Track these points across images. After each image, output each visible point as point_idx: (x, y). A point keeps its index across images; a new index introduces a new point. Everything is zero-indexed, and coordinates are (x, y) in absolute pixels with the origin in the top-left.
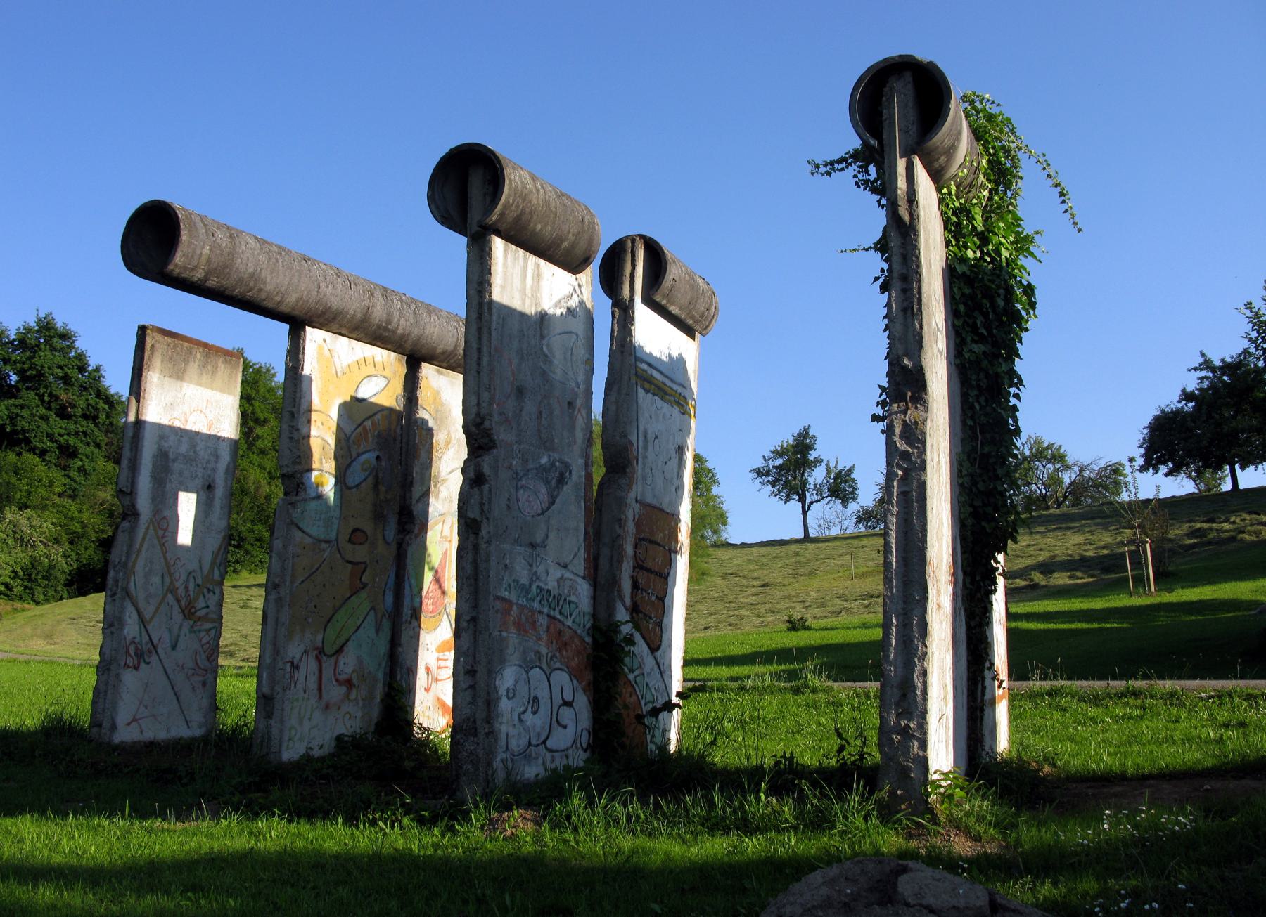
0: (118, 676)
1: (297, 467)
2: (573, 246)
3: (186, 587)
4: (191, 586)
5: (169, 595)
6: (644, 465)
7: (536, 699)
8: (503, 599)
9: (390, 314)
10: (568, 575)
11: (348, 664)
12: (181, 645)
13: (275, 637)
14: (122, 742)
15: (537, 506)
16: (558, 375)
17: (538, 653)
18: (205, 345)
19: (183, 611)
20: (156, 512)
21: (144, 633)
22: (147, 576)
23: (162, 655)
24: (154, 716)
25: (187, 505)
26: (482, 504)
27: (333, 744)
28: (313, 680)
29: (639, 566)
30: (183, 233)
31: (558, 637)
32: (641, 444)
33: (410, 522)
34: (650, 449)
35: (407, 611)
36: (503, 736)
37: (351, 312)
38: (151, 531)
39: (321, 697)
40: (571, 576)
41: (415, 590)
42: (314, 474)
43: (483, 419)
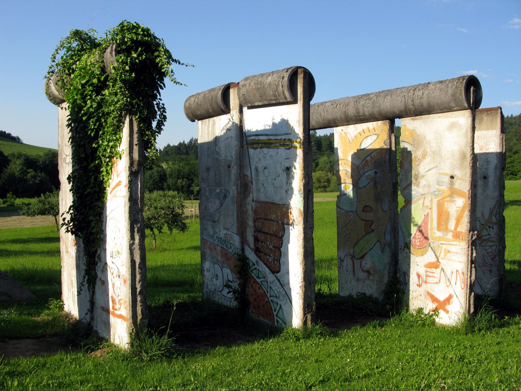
2: (213, 109)
6: (257, 185)
7: (217, 275)
8: (204, 239)
10: (228, 233)
11: (367, 263)
15: (215, 207)
16: (222, 157)
28: (350, 268)
29: (257, 230)
31: (225, 254)
32: (253, 174)
34: (261, 175)
35: (401, 244)
37: (339, 117)
39: (354, 275)
40: (231, 233)
42: (343, 185)
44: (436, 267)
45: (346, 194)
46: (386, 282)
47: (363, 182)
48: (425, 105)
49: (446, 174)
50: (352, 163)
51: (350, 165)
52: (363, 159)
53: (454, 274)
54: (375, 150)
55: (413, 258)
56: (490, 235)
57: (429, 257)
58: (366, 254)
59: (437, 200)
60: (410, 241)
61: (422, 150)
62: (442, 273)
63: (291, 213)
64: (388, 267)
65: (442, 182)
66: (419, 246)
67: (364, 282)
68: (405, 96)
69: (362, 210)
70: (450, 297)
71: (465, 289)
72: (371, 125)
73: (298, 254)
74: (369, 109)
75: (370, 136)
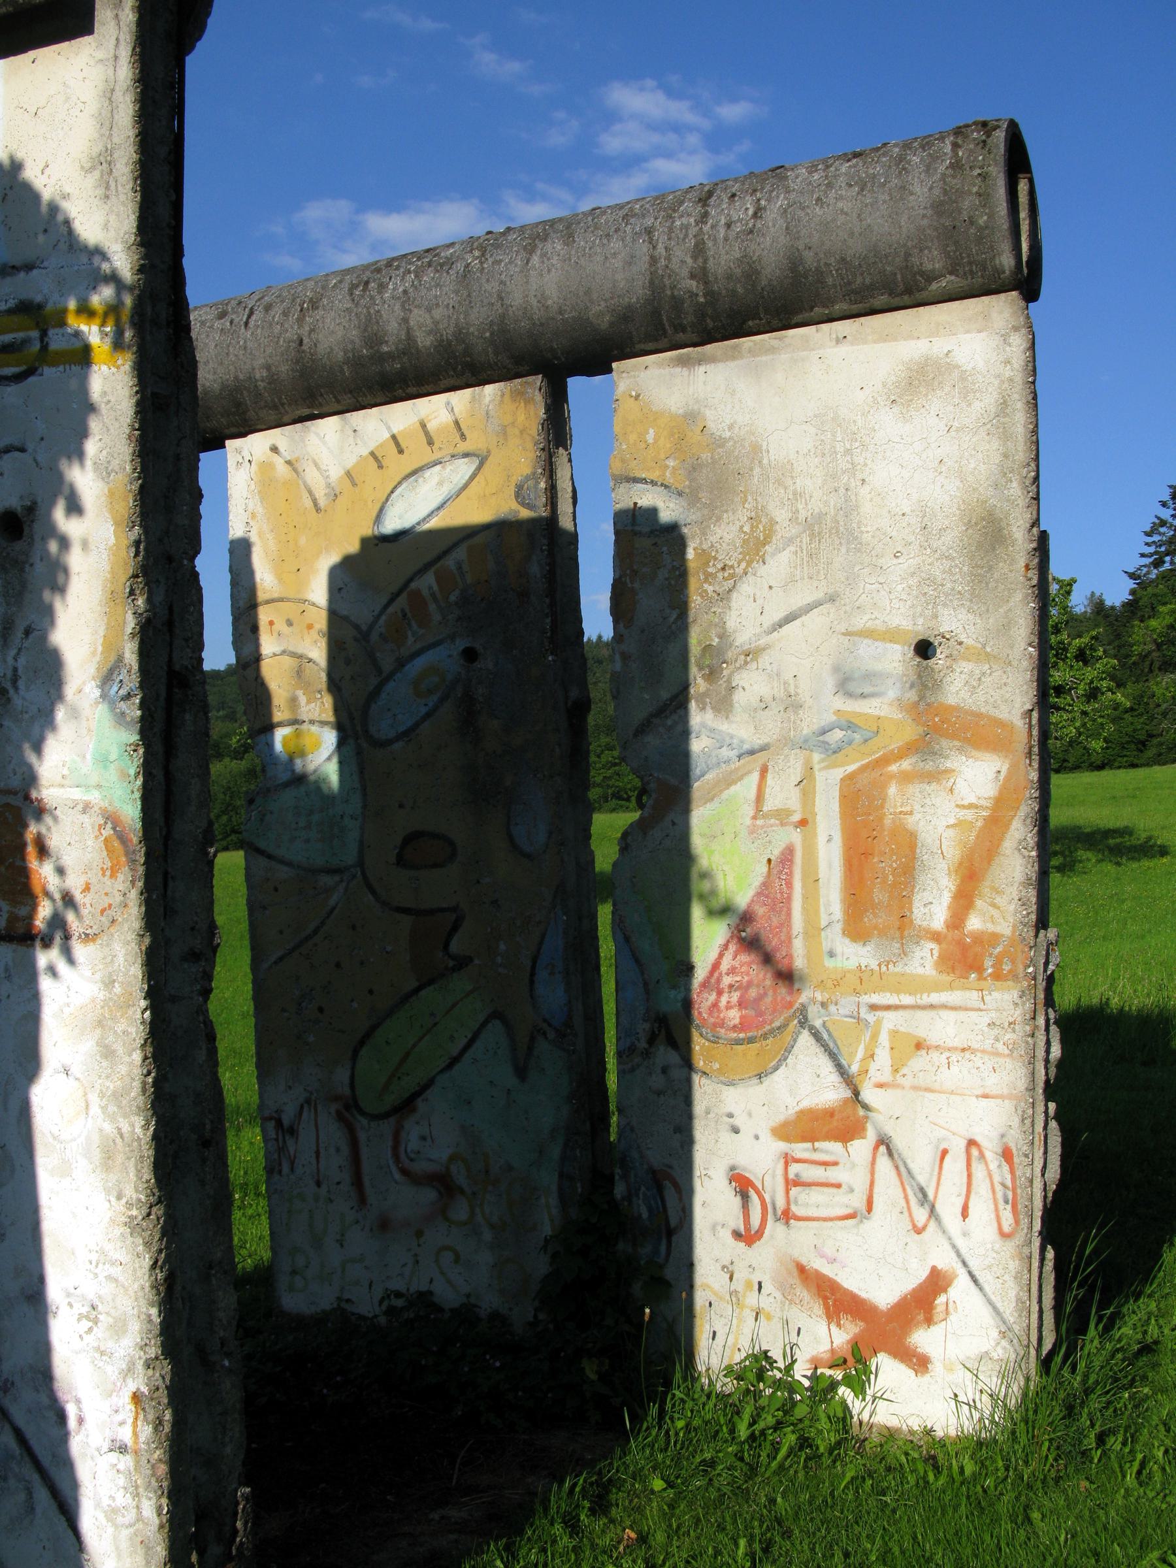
11: (435, 1136)
28: (335, 1165)
39: (362, 1200)
42: (280, 735)
45: (300, 779)
46: (547, 1230)
47: (400, 706)
48: (772, 265)
49: (891, 635)
50: (335, 615)
51: (321, 621)
52: (398, 593)
53: (955, 1166)
54: (467, 534)
55: (707, 1095)
57: (805, 1080)
59: (839, 773)
60: (687, 1004)
61: (743, 515)
62: (883, 1163)
63: (43, 851)
64: (556, 1151)
65: (869, 676)
66: (742, 1026)
67: (419, 1234)
68: (649, 231)
70: (936, 1282)
71: (1019, 1238)
72: (437, 409)
73: (108, 1156)
74: (437, 313)
75: (434, 464)
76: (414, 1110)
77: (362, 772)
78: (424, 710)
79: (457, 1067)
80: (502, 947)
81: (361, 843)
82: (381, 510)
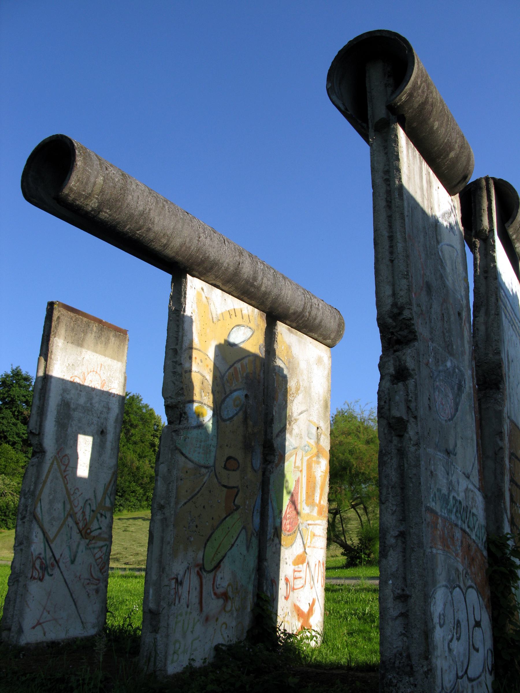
0: (25, 586)
1: (180, 398)
3: (84, 512)
4: (88, 511)
5: (70, 519)
9: (255, 272)
11: (224, 578)
12: (79, 559)
13: (161, 555)
14: (27, 644)
17: (457, 570)
18: (100, 322)
19: (80, 532)
20: (59, 450)
21: (48, 550)
22: (51, 502)
23: (62, 569)
24: (55, 620)
25: (85, 445)
26: (408, 401)
27: (213, 654)
30: (78, 158)
33: (271, 453)
35: (270, 530)
36: (439, 673)
37: (225, 265)
38: (55, 466)
39: (201, 610)
41: (277, 512)
42: (195, 405)
43: (401, 309)
44: (302, 562)
51: (211, 366)
56: (100, 528)
58: (224, 557)
67: (217, 620)
69: (223, 465)
76: (220, 567)
77: (218, 428)
78: (235, 412)
79: (233, 548)
80: (247, 502)
81: (215, 457)
82: (230, 333)
